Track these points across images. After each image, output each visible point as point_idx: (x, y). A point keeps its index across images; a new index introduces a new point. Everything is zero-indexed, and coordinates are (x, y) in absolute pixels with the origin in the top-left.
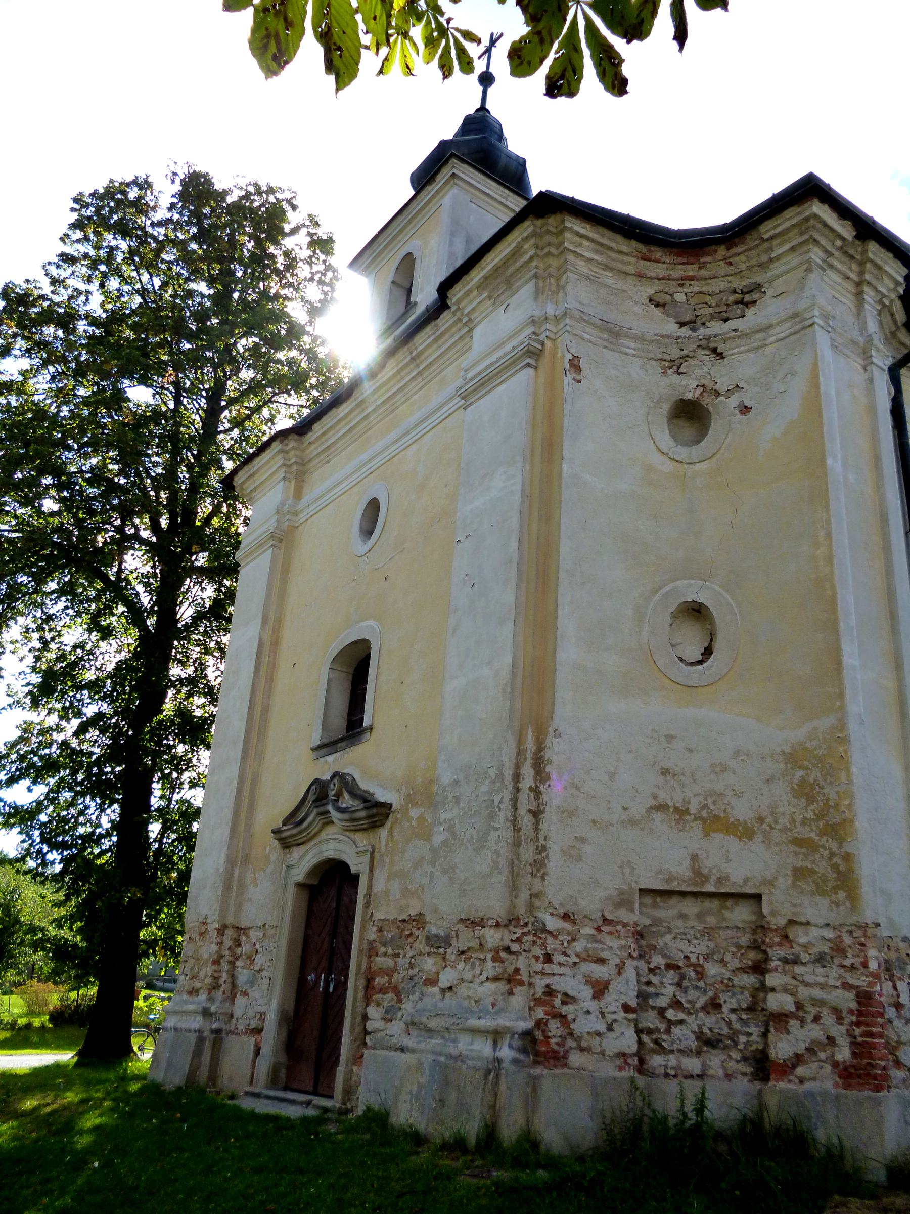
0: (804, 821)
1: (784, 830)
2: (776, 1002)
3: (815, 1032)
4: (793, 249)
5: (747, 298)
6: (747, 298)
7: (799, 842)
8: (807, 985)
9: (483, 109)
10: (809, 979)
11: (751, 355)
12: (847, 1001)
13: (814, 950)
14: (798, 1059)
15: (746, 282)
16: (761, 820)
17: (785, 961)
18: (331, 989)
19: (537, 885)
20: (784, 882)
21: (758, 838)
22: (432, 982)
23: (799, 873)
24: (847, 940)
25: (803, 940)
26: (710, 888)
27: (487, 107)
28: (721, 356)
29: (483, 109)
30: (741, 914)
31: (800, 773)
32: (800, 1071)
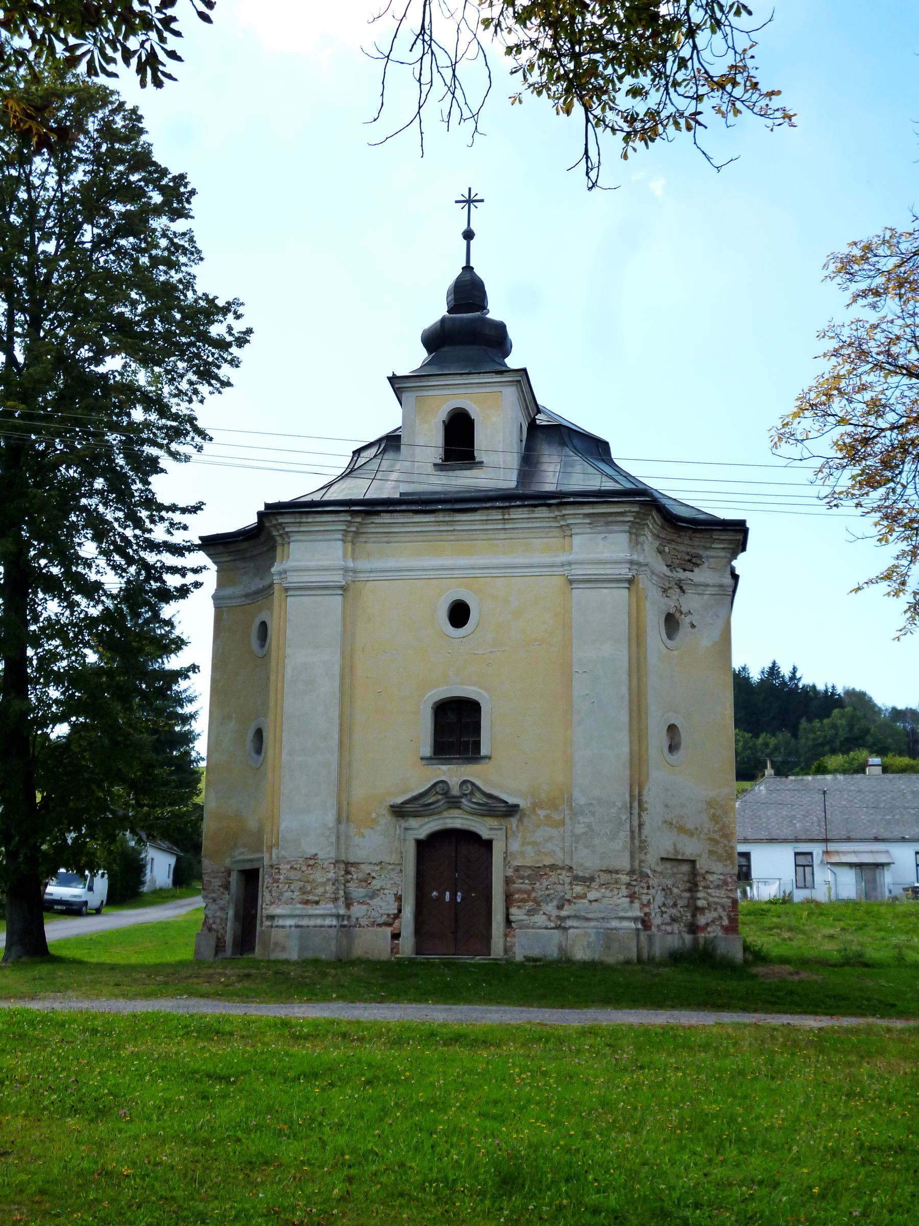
0: (714, 831)
1: (706, 834)
2: (700, 903)
3: (714, 914)
4: (724, 548)
5: (694, 560)
6: (694, 560)
7: (711, 839)
8: (713, 897)
9: (468, 268)
10: (714, 894)
11: (697, 596)
12: (728, 902)
13: (716, 883)
14: (707, 925)
15: (693, 551)
16: (697, 829)
17: (704, 887)
18: (459, 900)
19: (643, 857)
20: (705, 856)
21: (695, 836)
22: (584, 896)
23: (711, 852)
24: (729, 880)
25: (711, 879)
26: (680, 857)
27: (471, 265)
28: (683, 591)
29: (468, 268)
30: (685, 868)
31: (713, 811)
32: (709, 929)
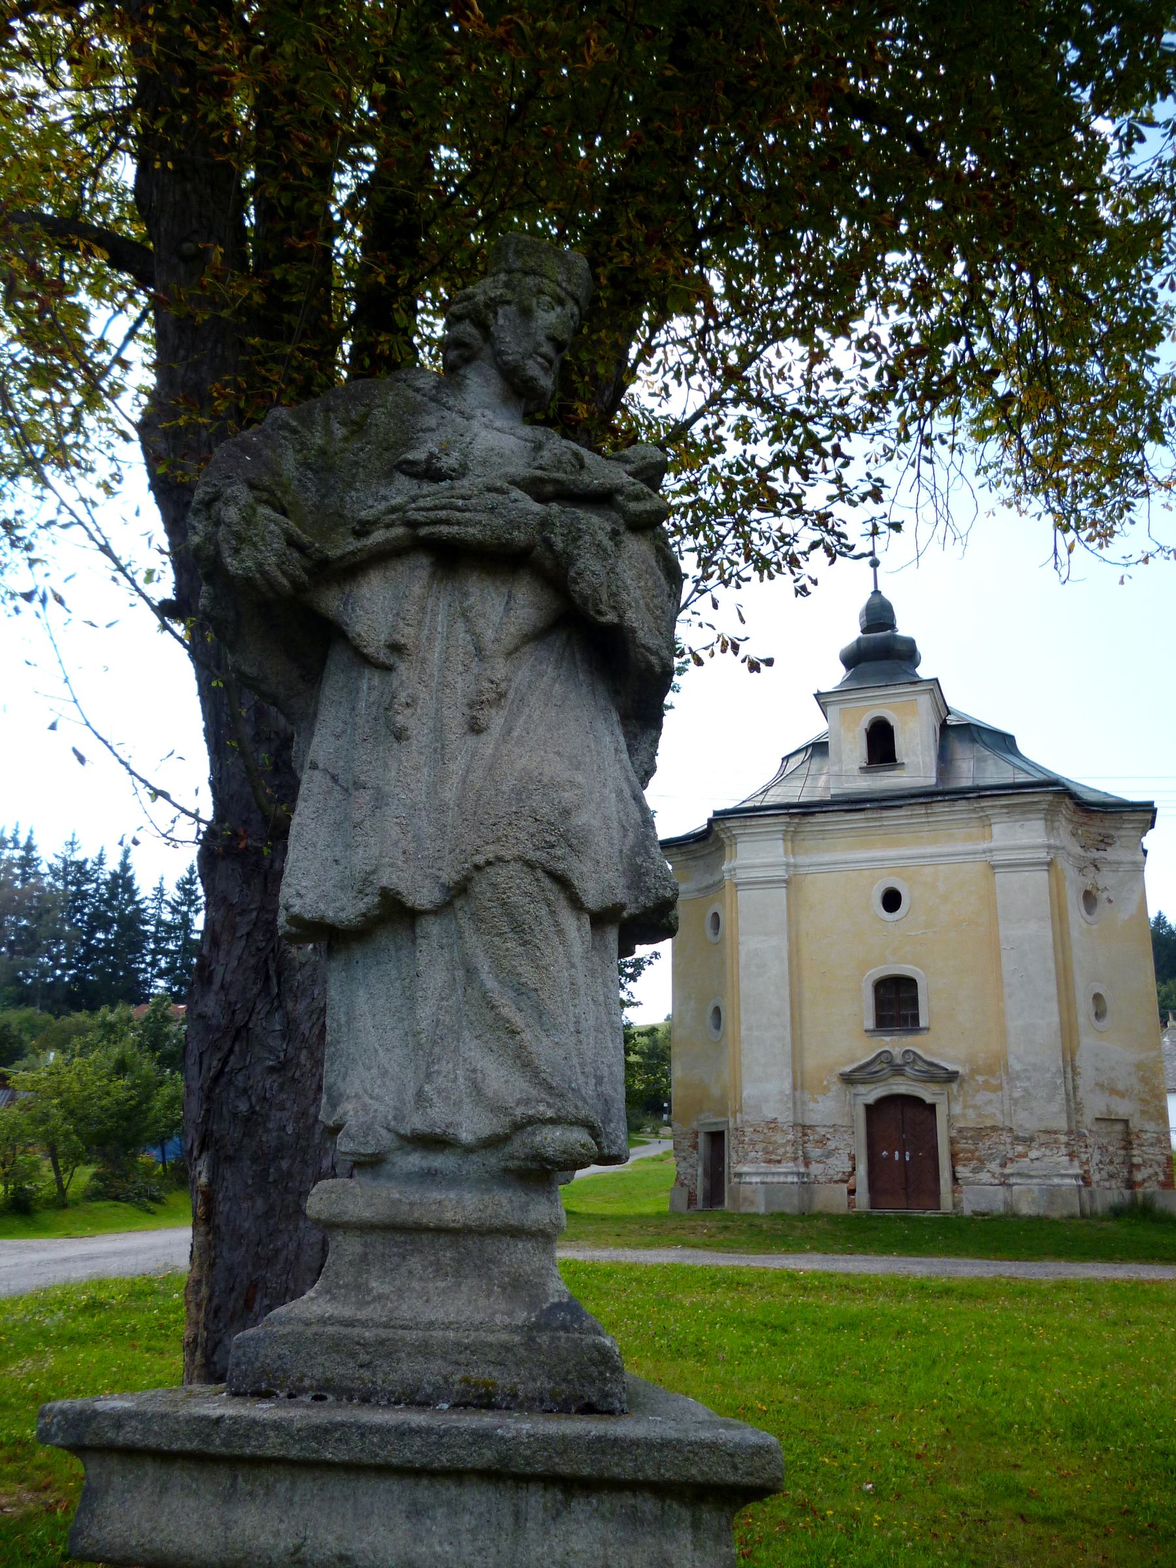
2: (1136, 1160)
3: (1151, 1171)
7: (1143, 1100)
9: (876, 592)
12: (1162, 1159)
14: (1144, 1180)
20: (1137, 1115)
22: (1025, 1155)
23: (1143, 1112)
29: (876, 592)
30: (1119, 1127)
